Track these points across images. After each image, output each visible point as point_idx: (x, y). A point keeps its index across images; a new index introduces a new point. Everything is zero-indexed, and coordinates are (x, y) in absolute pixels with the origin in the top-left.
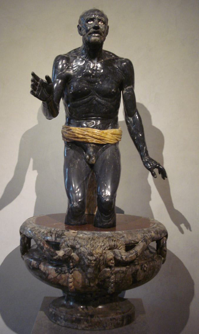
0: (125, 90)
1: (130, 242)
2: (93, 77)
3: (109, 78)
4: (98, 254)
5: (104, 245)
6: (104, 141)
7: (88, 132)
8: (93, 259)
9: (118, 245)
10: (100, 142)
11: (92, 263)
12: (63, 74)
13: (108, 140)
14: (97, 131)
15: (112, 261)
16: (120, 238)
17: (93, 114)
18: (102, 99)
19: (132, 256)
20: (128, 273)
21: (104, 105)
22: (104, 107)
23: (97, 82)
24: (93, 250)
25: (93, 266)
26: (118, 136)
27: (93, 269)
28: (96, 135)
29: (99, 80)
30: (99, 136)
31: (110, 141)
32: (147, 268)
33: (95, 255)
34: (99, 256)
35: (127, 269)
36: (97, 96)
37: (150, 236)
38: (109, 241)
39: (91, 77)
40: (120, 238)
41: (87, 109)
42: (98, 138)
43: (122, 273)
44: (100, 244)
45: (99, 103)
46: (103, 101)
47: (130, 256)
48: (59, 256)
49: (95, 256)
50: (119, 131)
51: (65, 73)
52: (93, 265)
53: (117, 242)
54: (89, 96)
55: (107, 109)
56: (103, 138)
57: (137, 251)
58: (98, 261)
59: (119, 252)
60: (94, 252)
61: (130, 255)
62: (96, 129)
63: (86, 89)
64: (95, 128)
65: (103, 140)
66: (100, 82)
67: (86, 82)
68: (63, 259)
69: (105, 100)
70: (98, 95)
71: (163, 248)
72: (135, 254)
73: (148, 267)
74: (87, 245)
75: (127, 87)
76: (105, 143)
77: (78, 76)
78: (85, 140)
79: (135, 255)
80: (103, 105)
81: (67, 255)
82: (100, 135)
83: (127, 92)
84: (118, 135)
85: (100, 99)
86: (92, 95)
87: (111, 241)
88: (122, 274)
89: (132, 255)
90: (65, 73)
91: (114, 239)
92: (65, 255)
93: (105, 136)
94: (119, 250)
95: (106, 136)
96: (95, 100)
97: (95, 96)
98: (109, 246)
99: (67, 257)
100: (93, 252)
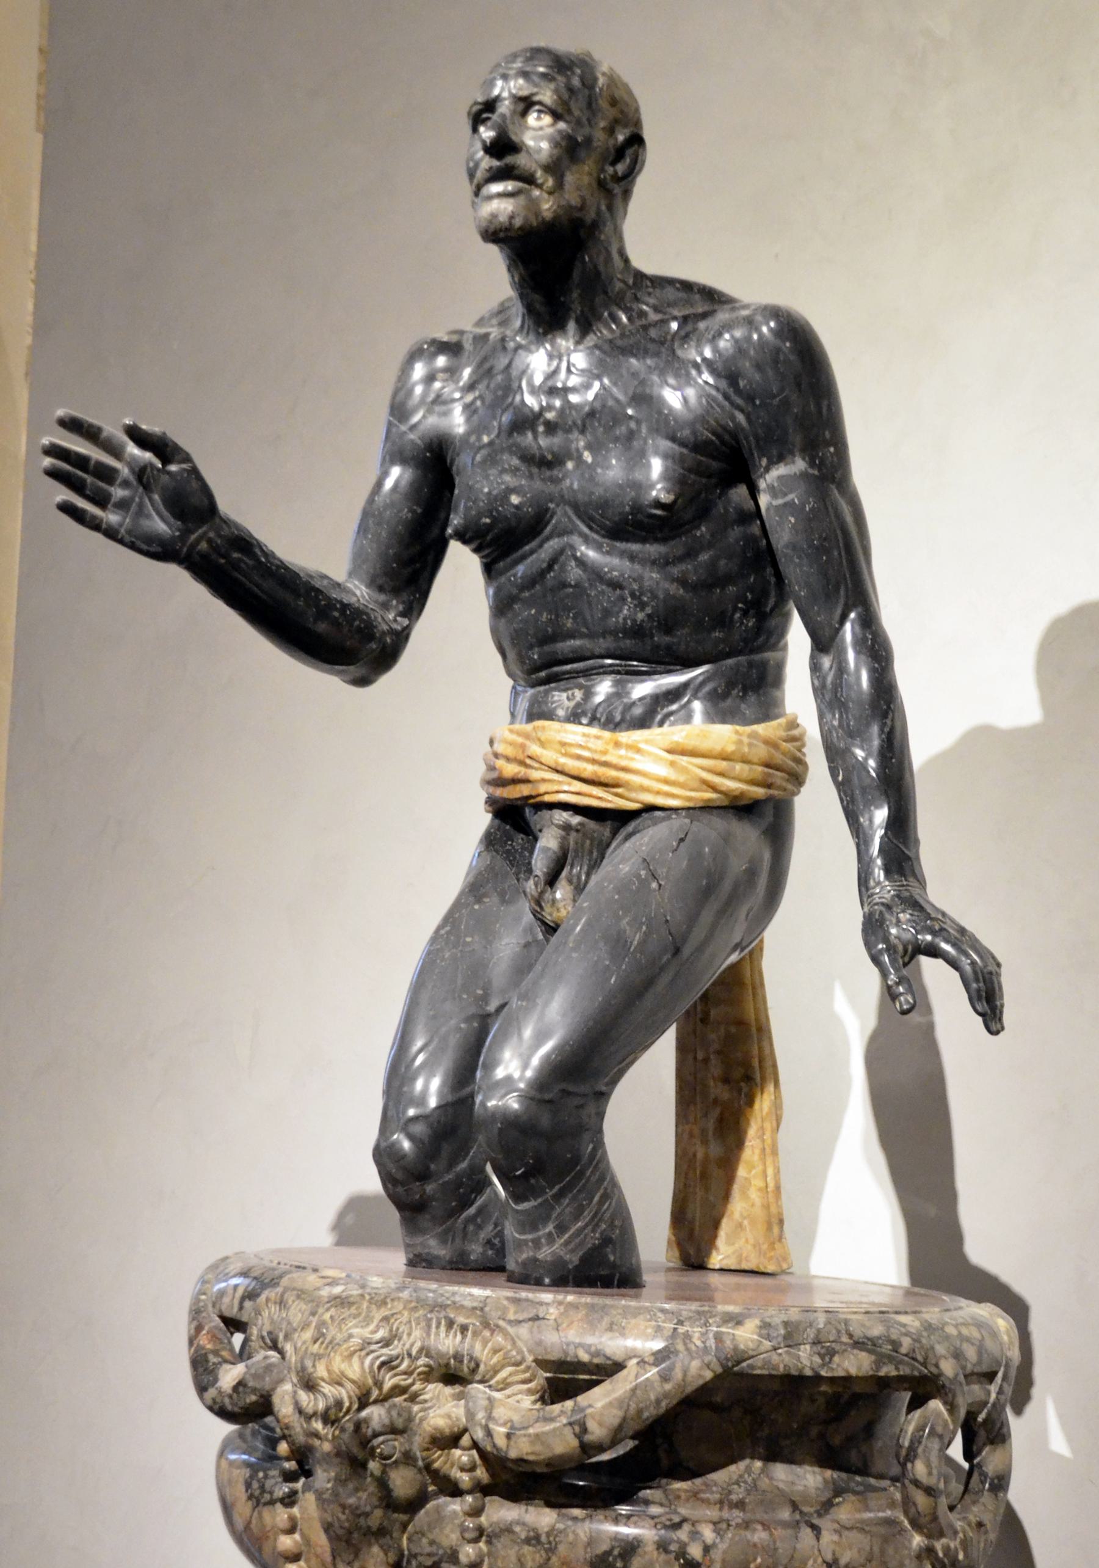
0: (764, 491)
1: (566, 1353)
2: (551, 428)
3: (633, 425)
4: (340, 1384)
5: (386, 1343)
6: (619, 790)
7: (542, 744)
8: (316, 1404)
9: (484, 1359)
10: (600, 798)
11: (316, 1435)
12: (412, 436)
13: (646, 782)
14: (584, 735)
15: (457, 1452)
16: (510, 1322)
17: (576, 643)
18: (608, 553)
19: (543, 1433)
20: (562, 1549)
21: (621, 588)
22: (623, 599)
23: (571, 458)
24: (318, 1357)
25: (328, 1454)
26: (723, 765)
27: (333, 1474)
28: (579, 758)
29: (582, 444)
30: (594, 761)
31: (658, 793)
32: (707, 1549)
33: (327, 1389)
34: (350, 1397)
35: (560, 1526)
36: (582, 535)
37: (711, 1343)
38: (429, 1326)
39: (541, 429)
40: (510, 1322)
41: (545, 616)
42: (585, 775)
43: (528, 1541)
44: (366, 1332)
45: (596, 574)
46: (616, 561)
47: (531, 1431)
48: (220, 1392)
49: (324, 1395)
50: (735, 737)
51: (422, 427)
52: (327, 1447)
53: (475, 1334)
54: (548, 539)
55: (642, 606)
56: (613, 773)
57: (582, 1410)
58: (350, 1427)
59: (489, 1399)
60: (321, 1371)
61: (537, 1421)
62: (589, 724)
63: (515, 500)
64: (585, 721)
65: (616, 785)
66: (588, 457)
67: (515, 461)
68: (236, 1409)
69: (622, 554)
70: (586, 530)
71: (909, 1465)
72: (565, 1421)
73: (723, 1546)
74: (303, 1329)
75: (767, 469)
76: (634, 806)
77: (479, 439)
78: (524, 790)
79: (568, 1431)
80: (615, 585)
81: (254, 1390)
82: (597, 757)
83: (775, 503)
84: (725, 757)
85: (598, 547)
86: (560, 535)
87: (438, 1326)
88: (527, 1549)
89: (548, 1427)
90: (422, 427)
91: (461, 1320)
92: (241, 1389)
93: (624, 763)
94: (490, 1387)
95: (633, 765)
96: (576, 559)
97: (576, 539)
98: (425, 1351)
99: (254, 1398)
100: (314, 1366)
